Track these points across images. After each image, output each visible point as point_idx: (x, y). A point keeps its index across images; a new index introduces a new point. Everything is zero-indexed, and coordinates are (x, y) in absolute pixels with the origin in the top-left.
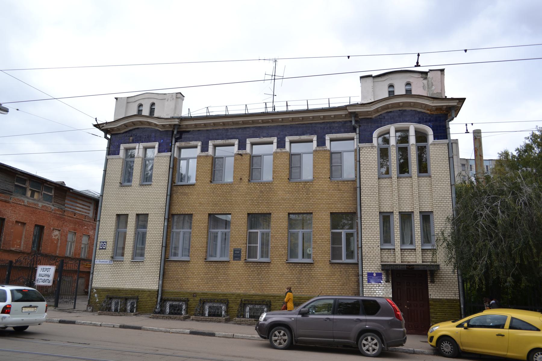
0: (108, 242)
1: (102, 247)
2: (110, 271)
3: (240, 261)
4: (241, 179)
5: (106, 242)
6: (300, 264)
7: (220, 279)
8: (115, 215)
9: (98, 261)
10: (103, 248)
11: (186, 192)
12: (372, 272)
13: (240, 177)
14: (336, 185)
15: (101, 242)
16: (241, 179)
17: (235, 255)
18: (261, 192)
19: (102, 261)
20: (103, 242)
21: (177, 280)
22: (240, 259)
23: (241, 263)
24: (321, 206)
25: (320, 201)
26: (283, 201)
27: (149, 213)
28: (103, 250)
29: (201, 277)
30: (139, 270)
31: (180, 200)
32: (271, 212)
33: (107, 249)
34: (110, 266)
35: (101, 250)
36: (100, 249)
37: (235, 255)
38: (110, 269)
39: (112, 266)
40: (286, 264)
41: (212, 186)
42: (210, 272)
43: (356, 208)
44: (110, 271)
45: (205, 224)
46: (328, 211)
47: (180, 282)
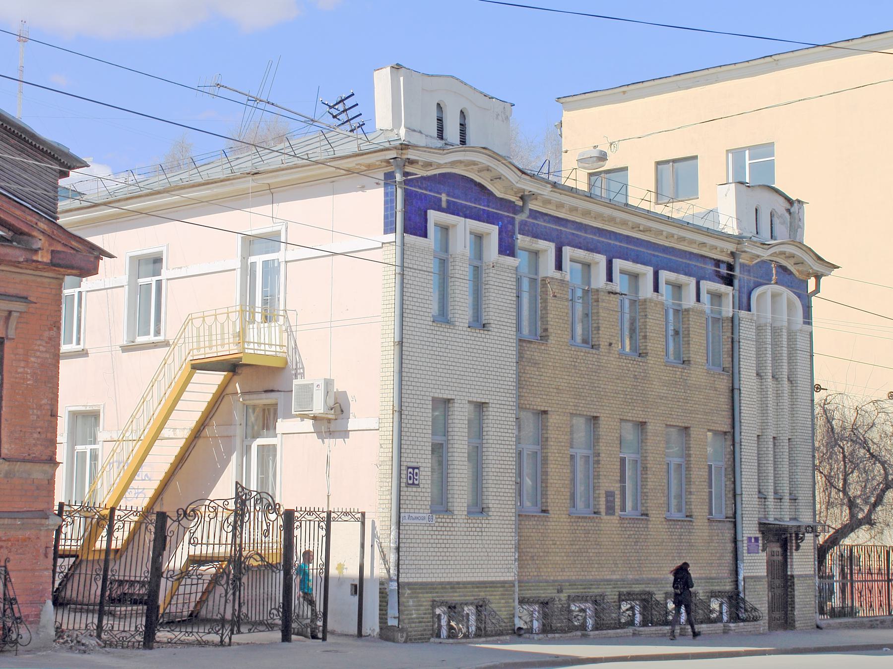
0: (421, 469)
1: (411, 482)
2: (432, 541)
3: (615, 517)
4: (610, 344)
5: (418, 468)
6: (680, 523)
7: (591, 554)
8: (430, 398)
9: (407, 515)
10: (413, 484)
11: (537, 358)
12: (751, 536)
13: (608, 340)
14: (712, 379)
15: (409, 468)
16: (610, 344)
17: (609, 504)
18: (635, 377)
19: (414, 515)
20: (414, 468)
21: (532, 558)
22: (613, 514)
23: (615, 519)
24: (699, 416)
25: (697, 406)
26: (659, 401)
27: (491, 401)
28: (414, 489)
29: (565, 550)
30: (483, 538)
31: (528, 376)
32: (647, 420)
33: (421, 486)
34: (430, 528)
35: (410, 489)
36: (408, 485)
37: (609, 504)
38: (430, 537)
39: (434, 528)
40: (664, 523)
41: (572, 352)
42: (578, 539)
43: (733, 427)
44: (432, 541)
45: (566, 437)
46: (706, 427)
47: (538, 562)
